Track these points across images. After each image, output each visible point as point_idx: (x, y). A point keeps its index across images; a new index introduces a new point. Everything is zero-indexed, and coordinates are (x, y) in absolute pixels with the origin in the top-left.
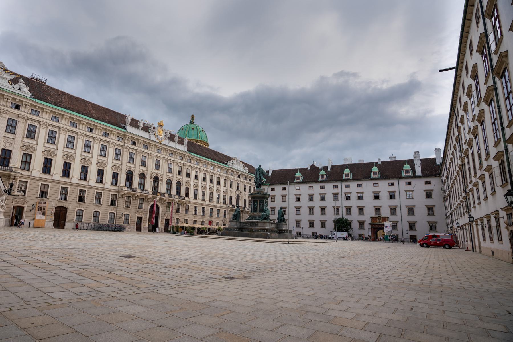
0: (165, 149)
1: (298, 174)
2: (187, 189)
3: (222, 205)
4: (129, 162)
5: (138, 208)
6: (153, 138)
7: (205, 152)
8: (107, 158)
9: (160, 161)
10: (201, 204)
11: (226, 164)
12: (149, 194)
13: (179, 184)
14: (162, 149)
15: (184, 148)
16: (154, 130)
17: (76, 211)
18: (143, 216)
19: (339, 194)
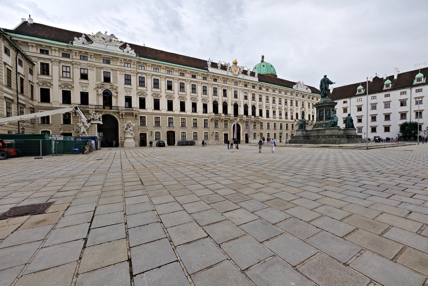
0: (240, 81)
2: (261, 111)
4: (214, 95)
6: (230, 74)
10: (272, 121)
11: (292, 88)
12: (231, 117)
13: (254, 108)
14: (238, 82)
15: (256, 79)
17: (181, 133)
18: (228, 133)
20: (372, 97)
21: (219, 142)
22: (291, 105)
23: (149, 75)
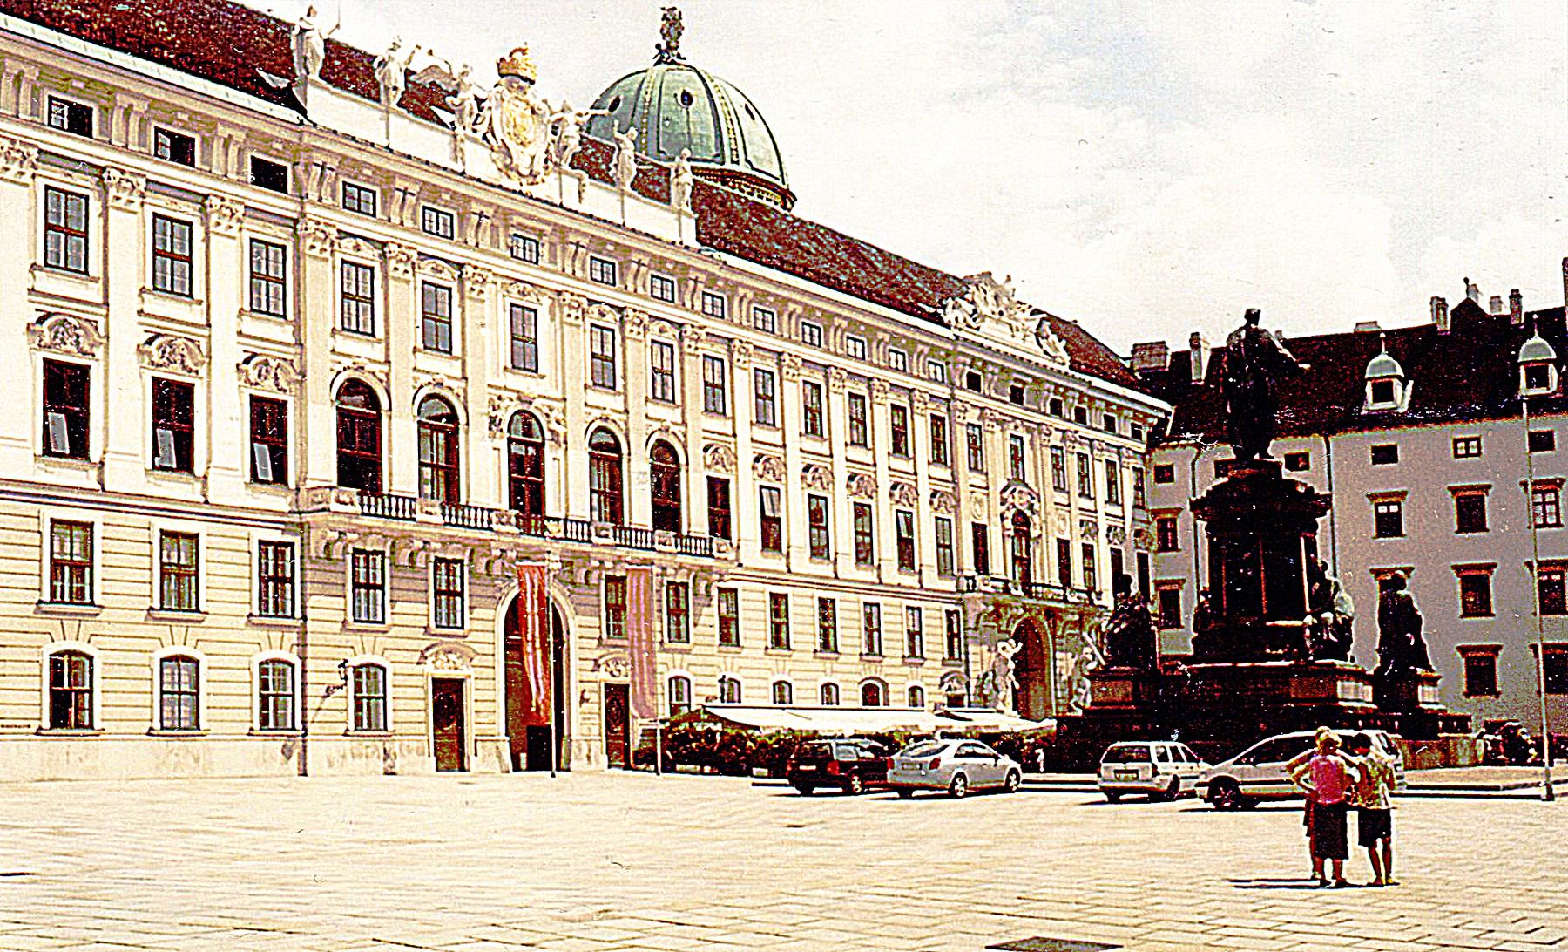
0: (562, 231)
1: (1383, 364)
2: (719, 492)
3: (932, 580)
6: (480, 162)
9: (535, 311)
10: (806, 583)
11: (936, 319)
13: (665, 455)
14: (542, 233)
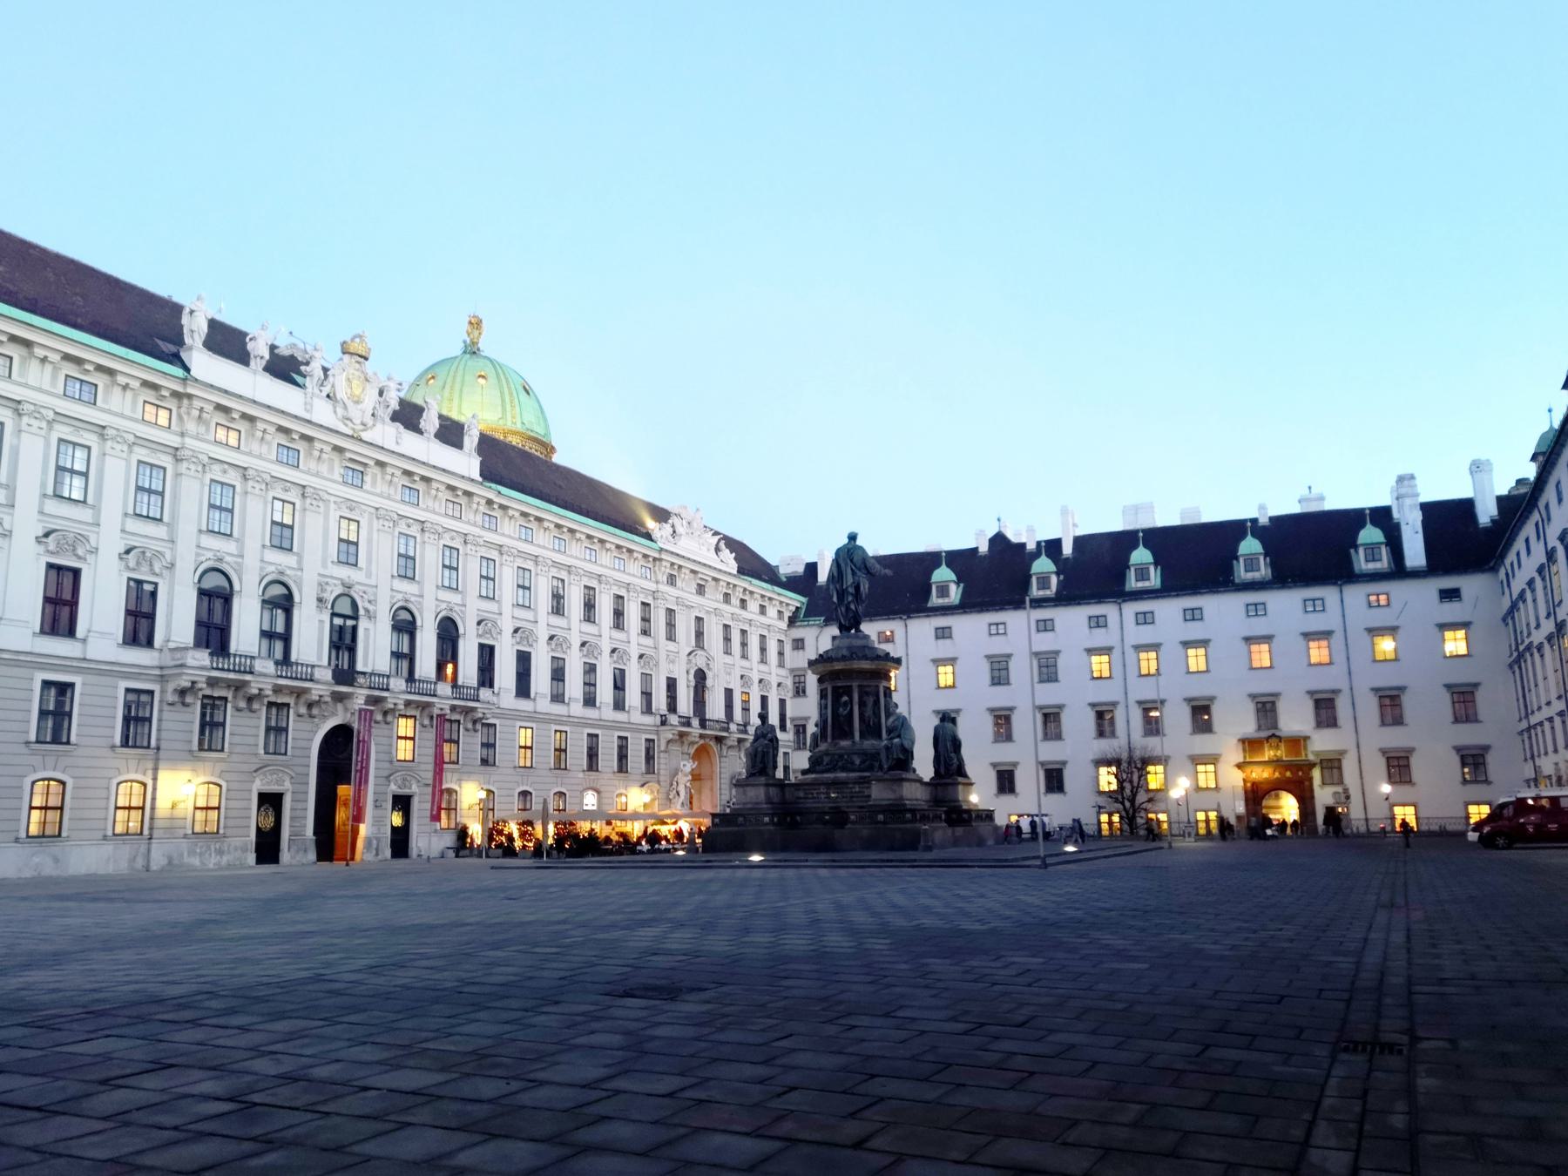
5: (262, 752)
6: (323, 413)
7: (555, 484)
8: (93, 507)
12: (317, 682)
14: (365, 465)
15: (466, 463)
16: (326, 376)
18: (286, 787)
19: (1114, 651)
20: (990, 625)
21: (220, 852)
22: (645, 632)
23: (37, 413)
